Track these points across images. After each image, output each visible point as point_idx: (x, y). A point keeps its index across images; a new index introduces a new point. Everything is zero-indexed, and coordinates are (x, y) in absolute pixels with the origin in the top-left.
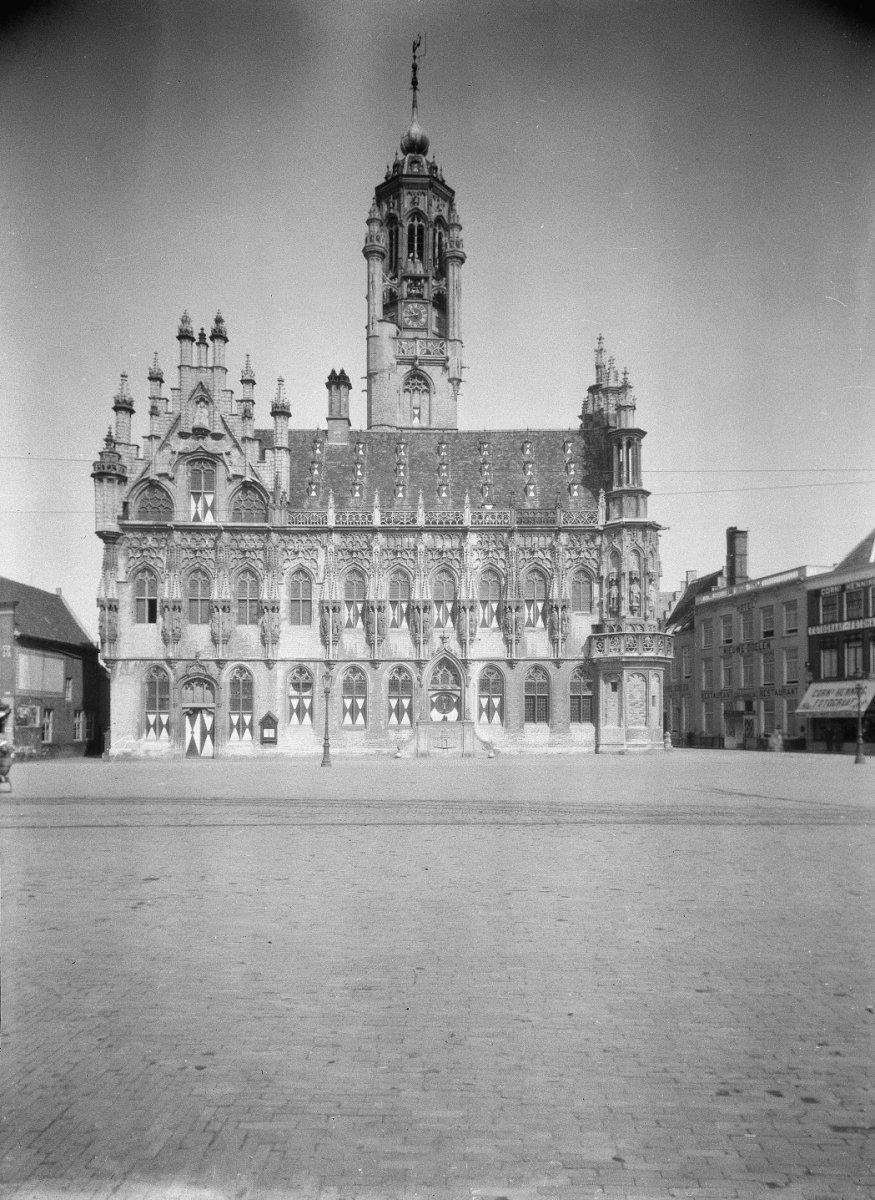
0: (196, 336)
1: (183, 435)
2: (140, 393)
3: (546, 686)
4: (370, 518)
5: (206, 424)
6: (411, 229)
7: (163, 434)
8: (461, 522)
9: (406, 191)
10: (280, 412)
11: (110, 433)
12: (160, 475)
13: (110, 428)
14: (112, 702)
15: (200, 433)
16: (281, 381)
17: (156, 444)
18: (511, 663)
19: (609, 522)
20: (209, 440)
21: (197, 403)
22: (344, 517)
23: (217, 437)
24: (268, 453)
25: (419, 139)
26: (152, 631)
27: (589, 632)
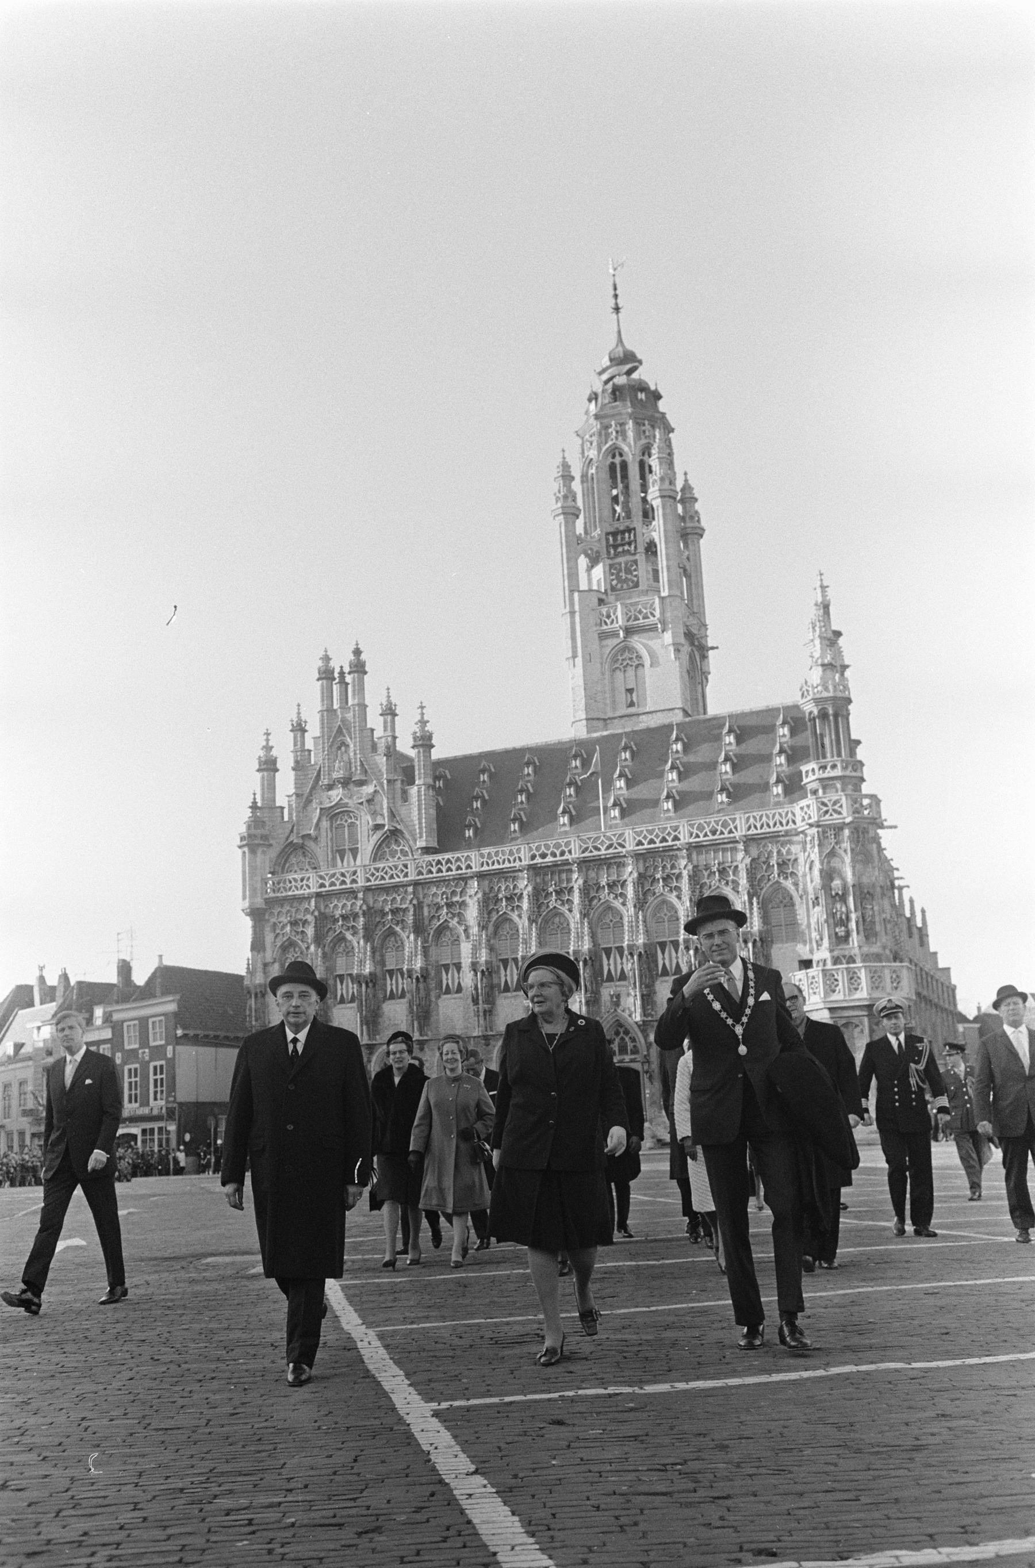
0: (336, 675)
10: (424, 742)
12: (303, 837)
21: (339, 748)
23: (361, 783)
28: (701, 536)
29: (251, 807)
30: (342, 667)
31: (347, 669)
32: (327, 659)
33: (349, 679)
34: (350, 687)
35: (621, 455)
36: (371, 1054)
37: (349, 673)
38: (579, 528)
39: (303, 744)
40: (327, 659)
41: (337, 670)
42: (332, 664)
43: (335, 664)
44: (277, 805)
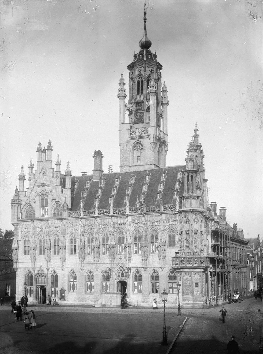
0: (43, 150)
1: (39, 186)
2: (26, 172)
3: (157, 278)
4: (95, 213)
5: (45, 182)
6: (138, 82)
7: (32, 187)
8: (126, 213)
9: (136, 67)
11: (17, 188)
13: (17, 187)
14: (17, 283)
15: (43, 185)
16: (68, 163)
17: (30, 190)
18: (145, 269)
19: (180, 209)
20: (46, 187)
22: (86, 213)
23: (49, 186)
24: (64, 190)
25: (144, 42)
26: (28, 258)
27: (174, 255)
28: (168, 104)
29: (15, 191)
30: (44, 147)
31: (46, 148)
32: (40, 145)
33: (46, 151)
34: (47, 154)
35: (141, 78)
36: (48, 271)
37: (47, 150)
38: (127, 101)
39: (32, 171)
40: (40, 145)
41: (43, 148)
42: (42, 146)
43: (43, 146)
44: (25, 191)
